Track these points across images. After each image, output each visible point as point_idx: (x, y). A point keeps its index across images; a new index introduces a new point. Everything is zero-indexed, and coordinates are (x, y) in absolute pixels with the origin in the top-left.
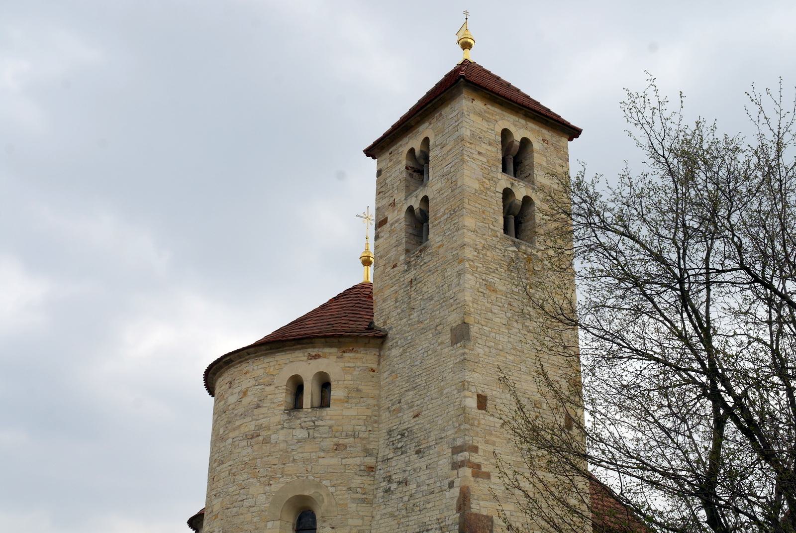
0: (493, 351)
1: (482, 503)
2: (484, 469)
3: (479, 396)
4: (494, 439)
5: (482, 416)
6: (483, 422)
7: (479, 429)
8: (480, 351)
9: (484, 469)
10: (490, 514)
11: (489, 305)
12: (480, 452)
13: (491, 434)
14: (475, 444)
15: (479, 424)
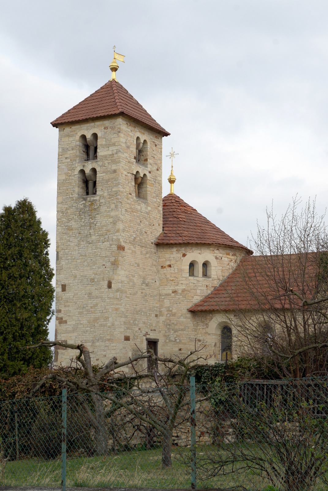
0: (70, 261)
1: (62, 335)
2: (64, 319)
3: (62, 285)
4: (69, 304)
5: (63, 295)
6: (64, 297)
7: (61, 301)
8: (63, 263)
9: (64, 319)
10: (66, 339)
11: (68, 238)
12: (62, 312)
13: (67, 302)
14: (60, 308)
15: (62, 299)
